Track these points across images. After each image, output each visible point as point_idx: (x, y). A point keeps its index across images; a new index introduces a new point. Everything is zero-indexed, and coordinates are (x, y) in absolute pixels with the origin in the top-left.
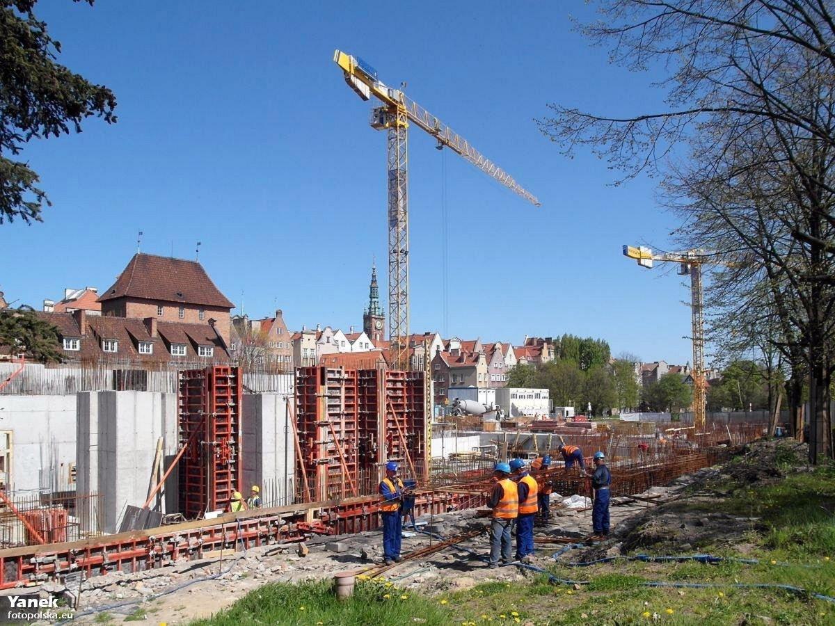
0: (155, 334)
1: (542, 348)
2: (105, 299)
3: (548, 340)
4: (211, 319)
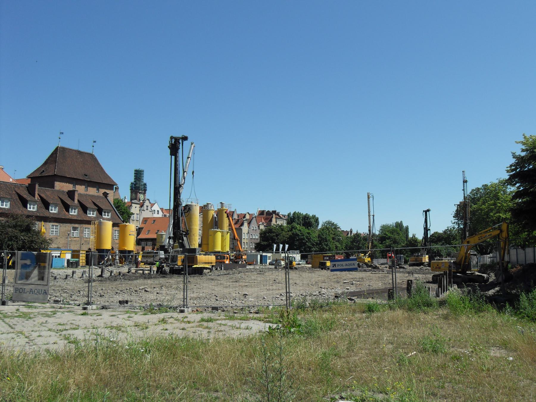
0: (76, 201)
1: (272, 217)
2: (38, 175)
3: (274, 212)
4: (105, 192)
